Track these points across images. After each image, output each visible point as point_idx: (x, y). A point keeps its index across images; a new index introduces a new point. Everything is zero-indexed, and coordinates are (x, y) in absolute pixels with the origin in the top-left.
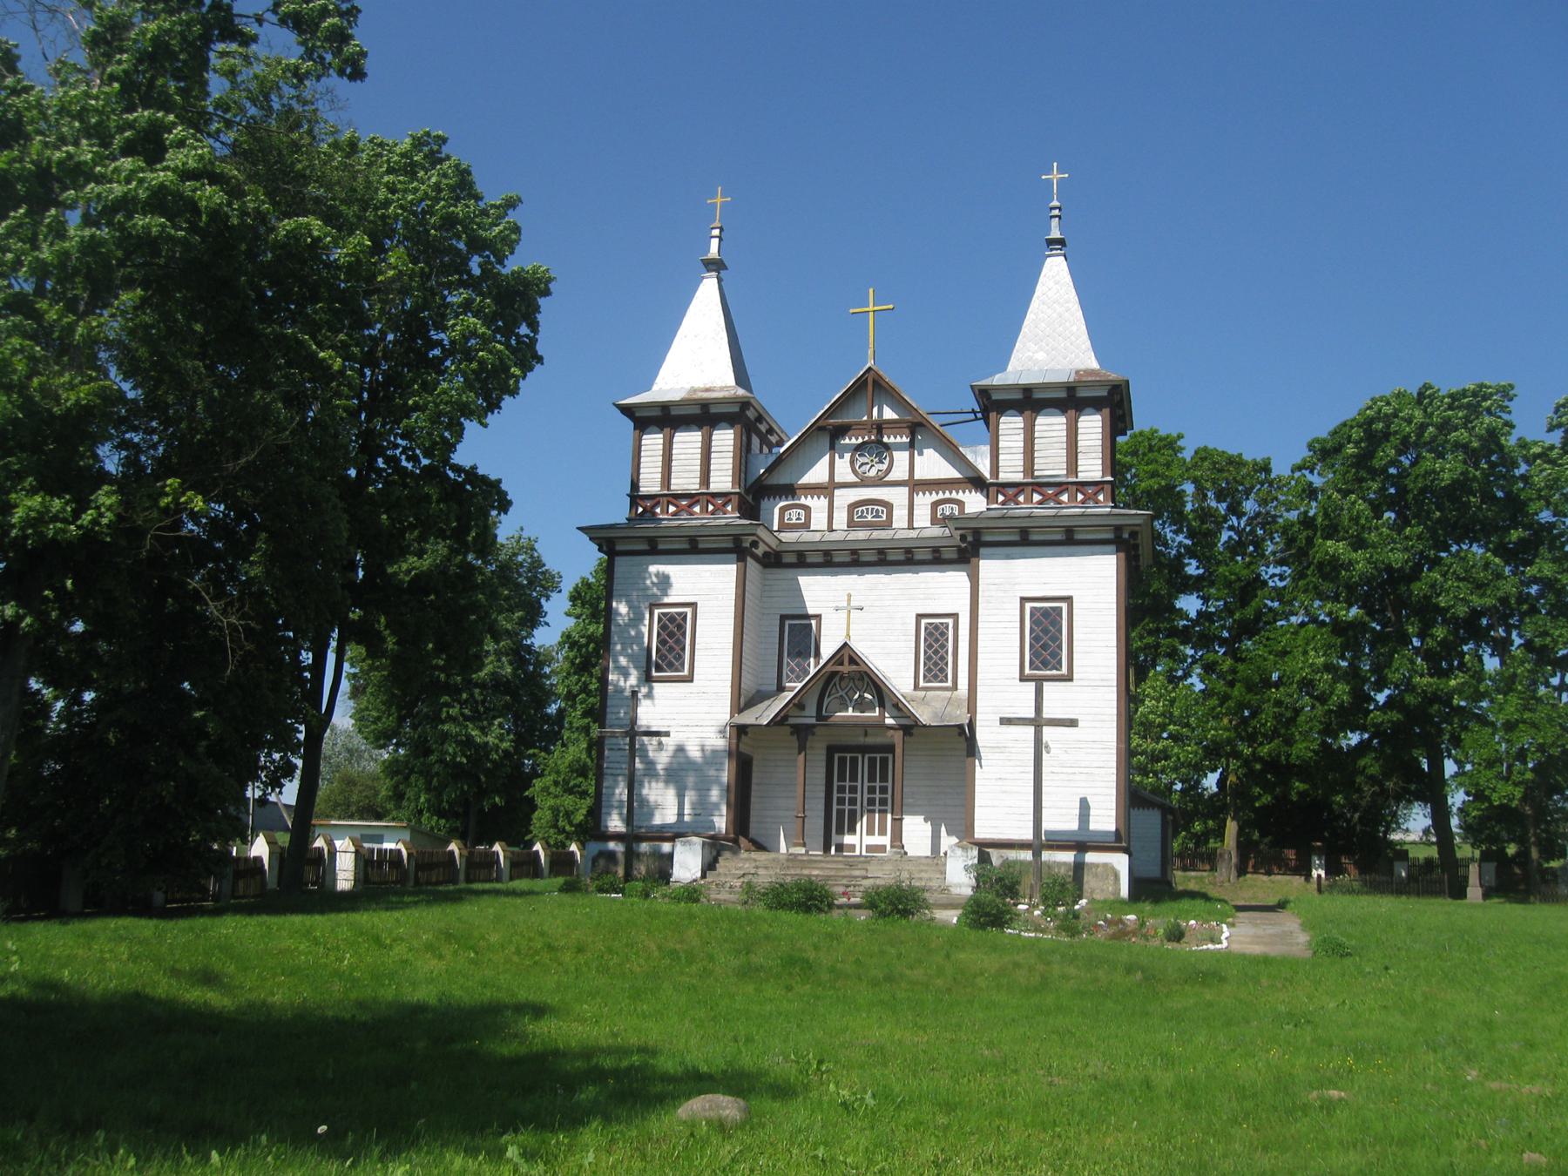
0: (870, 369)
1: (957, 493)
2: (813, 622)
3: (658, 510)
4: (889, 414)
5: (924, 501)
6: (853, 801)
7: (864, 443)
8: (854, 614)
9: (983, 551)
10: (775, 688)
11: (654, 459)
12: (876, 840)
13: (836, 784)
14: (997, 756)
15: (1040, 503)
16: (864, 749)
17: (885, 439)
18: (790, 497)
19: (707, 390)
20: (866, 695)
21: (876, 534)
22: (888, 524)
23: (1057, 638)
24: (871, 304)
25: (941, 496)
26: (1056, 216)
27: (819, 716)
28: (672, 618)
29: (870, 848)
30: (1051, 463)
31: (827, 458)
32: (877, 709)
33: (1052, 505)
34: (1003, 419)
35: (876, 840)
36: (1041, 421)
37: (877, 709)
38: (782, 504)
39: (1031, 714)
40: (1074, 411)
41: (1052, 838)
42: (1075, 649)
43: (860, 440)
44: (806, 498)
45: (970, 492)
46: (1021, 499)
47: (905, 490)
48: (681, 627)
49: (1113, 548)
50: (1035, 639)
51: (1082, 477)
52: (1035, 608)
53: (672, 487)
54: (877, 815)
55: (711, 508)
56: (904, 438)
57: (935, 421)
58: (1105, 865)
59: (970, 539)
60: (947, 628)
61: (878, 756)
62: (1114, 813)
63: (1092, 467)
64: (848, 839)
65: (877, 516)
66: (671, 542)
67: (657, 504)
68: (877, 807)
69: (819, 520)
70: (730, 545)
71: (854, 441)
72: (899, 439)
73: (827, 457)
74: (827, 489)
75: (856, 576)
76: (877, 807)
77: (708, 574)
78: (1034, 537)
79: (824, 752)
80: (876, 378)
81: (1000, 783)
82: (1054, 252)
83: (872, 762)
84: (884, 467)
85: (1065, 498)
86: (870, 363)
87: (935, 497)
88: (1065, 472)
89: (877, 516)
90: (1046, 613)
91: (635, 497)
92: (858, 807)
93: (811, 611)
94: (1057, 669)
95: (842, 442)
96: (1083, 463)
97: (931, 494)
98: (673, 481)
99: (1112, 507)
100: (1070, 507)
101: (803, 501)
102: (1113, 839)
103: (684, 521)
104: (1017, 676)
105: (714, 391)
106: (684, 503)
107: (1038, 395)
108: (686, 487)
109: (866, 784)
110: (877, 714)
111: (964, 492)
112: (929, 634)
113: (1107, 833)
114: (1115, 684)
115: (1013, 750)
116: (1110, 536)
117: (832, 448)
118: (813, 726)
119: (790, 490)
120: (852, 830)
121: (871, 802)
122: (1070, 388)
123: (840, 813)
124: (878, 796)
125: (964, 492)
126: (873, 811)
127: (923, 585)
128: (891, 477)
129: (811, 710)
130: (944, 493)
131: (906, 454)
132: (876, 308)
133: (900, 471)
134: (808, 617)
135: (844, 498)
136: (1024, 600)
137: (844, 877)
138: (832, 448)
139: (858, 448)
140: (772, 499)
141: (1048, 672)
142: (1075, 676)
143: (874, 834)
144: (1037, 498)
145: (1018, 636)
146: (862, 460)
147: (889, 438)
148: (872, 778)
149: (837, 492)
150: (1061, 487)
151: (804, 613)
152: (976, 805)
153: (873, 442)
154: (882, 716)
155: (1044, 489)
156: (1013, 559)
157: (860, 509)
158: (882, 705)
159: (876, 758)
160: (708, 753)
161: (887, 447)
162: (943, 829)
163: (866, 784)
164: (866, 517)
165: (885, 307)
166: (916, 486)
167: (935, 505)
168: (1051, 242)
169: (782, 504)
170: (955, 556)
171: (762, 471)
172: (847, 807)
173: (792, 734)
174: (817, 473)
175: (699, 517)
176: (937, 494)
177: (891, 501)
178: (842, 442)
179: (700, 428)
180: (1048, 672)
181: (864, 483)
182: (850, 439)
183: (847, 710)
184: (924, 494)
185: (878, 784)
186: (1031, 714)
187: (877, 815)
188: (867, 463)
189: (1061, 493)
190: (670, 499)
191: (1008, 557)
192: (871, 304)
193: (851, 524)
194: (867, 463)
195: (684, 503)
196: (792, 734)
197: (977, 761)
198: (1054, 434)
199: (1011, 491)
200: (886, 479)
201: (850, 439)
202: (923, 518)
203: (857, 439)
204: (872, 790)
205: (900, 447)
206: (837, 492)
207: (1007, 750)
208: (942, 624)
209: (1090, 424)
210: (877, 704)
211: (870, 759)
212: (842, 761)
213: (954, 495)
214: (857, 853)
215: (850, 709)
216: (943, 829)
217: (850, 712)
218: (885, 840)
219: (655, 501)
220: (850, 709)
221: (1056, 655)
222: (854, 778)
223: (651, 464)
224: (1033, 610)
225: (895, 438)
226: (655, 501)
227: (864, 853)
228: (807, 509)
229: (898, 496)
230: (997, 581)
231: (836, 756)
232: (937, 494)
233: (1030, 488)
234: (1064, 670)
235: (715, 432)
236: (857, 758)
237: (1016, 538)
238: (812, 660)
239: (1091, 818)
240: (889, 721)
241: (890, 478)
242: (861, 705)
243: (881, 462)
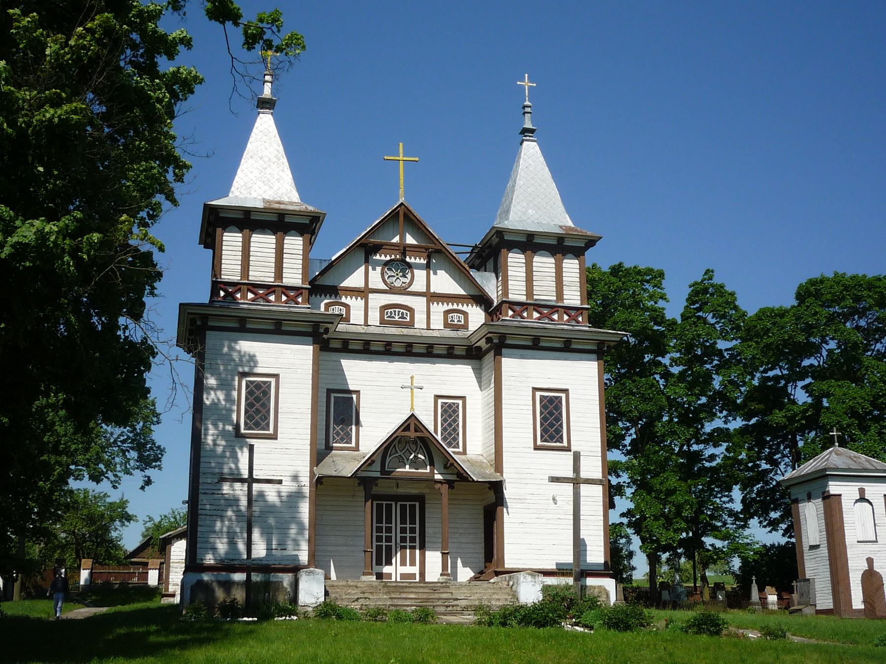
0: (402, 204)
1: (463, 305)
2: (354, 396)
3: (238, 296)
4: (410, 240)
5: (438, 309)
6: (389, 539)
7: (391, 260)
8: (415, 390)
9: (504, 351)
10: (324, 447)
11: (234, 253)
12: (408, 569)
13: (375, 525)
14: (519, 506)
15: (539, 319)
16: (397, 498)
17: (408, 259)
18: (333, 297)
19: (279, 203)
20: (420, 456)
21: (405, 331)
22: (411, 325)
23: (559, 419)
24: (401, 155)
25: (450, 307)
26: (528, 113)
27: (383, 471)
28: (258, 386)
29: (403, 576)
30: (545, 291)
31: (363, 268)
32: (428, 467)
33: (547, 321)
34: (510, 255)
35: (408, 569)
36: (537, 259)
37: (428, 467)
38: (326, 301)
39: (570, 474)
40: (530, 252)
41: (561, 567)
42: (572, 428)
43: (388, 258)
44: (346, 298)
45: (472, 306)
46: (525, 314)
48: (267, 393)
49: (594, 356)
50: (544, 419)
51: (567, 303)
52: (543, 396)
53: (250, 278)
54: (408, 551)
56: (422, 260)
57: (452, 249)
58: (600, 587)
59: (496, 341)
60: (458, 407)
62: (602, 549)
63: (573, 297)
64: (386, 569)
65: (402, 317)
66: (259, 323)
67: (239, 290)
68: (408, 544)
69: (357, 316)
70: (310, 330)
71: (383, 257)
72: (418, 261)
73: (363, 268)
74: (363, 293)
75: (387, 363)
76: (408, 544)
77: (289, 351)
78: (542, 344)
80: (406, 211)
81: (521, 526)
82: (528, 138)
83: (403, 508)
84: (407, 281)
85: (555, 317)
86: (402, 200)
87: (446, 307)
88: (555, 298)
89: (402, 317)
90: (551, 400)
91: (217, 285)
92: (393, 544)
93: (351, 388)
94: (560, 442)
95: (374, 258)
96: (566, 292)
97: (443, 304)
98: (251, 273)
99: (589, 327)
100: (560, 323)
101: (343, 300)
102: (603, 568)
103: (261, 306)
104: (532, 446)
105: (282, 204)
106: (261, 292)
107: (537, 240)
108: (262, 279)
109: (399, 526)
110: (428, 471)
111: (468, 305)
112: (444, 412)
113: (598, 565)
114: (600, 455)
115: (529, 501)
116: (594, 347)
117: (367, 261)
118: (377, 478)
119: (334, 291)
120: (389, 563)
121: (403, 539)
122: (560, 238)
124: (408, 535)
125: (468, 305)
126: (405, 548)
127: (438, 373)
128: (412, 289)
129: (377, 466)
130: (453, 305)
131: (424, 273)
132: (405, 159)
133: (419, 285)
134: (350, 392)
135: (377, 301)
136: (535, 389)
137: (439, 599)
138: (367, 261)
139: (386, 264)
140: (318, 296)
141: (554, 444)
143: (406, 566)
144: (536, 315)
145: (531, 416)
146: (390, 273)
147: (410, 258)
148: (403, 521)
149: (371, 296)
150: (554, 308)
151: (346, 388)
152: (505, 542)
153: (398, 260)
154: (433, 473)
155: (541, 309)
156: (526, 358)
157: (390, 310)
158: (432, 464)
160: (284, 499)
161: (410, 266)
162: (459, 561)
163: (399, 526)
164: (395, 318)
165: (391, 158)
166: (433, 297)
167: (447, 313)
168: (525, 131)
169: (326, 301)
170: (464, 353)
171: (317, 273)
172: (384, 544)
173: (359, 484)
174: (355, 280)
175: (277, 304)
176: (448, 304)
177: (413, 307)
178: (374, 258)
179: (241, 230)
180: (554, 444)
181: (392, 290)
182: (381, 256)
183: (405, 467)
184: (438, 304)
185: (408, 526)
186: (570, 474)
187: (408, 551)
188: (394, 276)
189: (553, 313)
190: (250, 287)
191: (522, 357)
192: (401, 155)
193: (383, 322)
194: (394, 276)
195: (261, 292)
196: (359, 484)
197: (505, 509)
198: (547, 270)
199: (518, 308)
200: (408, 290)
201: (381, 256)
202: (437, 322)
203: (386, 256)
204: (403, 530)
205: (419, 267)
206: (371, 296)
207: (527, 501)
208: (454, 404)
209: (570, 266)
210: (428, 463)
213: (460, 307)
214: (393, 579)
215: (407, 466)
216: (459, 561)
217: (407, 469)
218: (415, 570)
219: (237, 288)
220: (407, 466)
221: (559, 431)
222: (389, 521)
223: (231, 257)
225: (415, 259)
226: (237, 288)
227: (398, 580)
228: (347, 307)
229: (419, 304)
230: (515, 374)
232: (448, 304)
233: (532, 307)
234: (565, 444)
235: (253, 235)
237: (530, 343)
238: (354, 427)
239: (588, 553)
240: (438, 477)
242: (415, 464)
243: (404, 276)
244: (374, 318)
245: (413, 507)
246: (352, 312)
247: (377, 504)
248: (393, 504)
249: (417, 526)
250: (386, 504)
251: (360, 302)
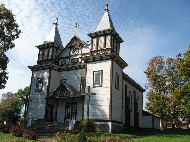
30: (101, 46)
42: (103, 80)
55: (48, 61)
69: (67, 63)
79: (65, 104)
123: (67, 115)
128: (79, 54)
141: (98, 85)
142: (103, 86)
180: (98, 85)
212: (68, 105)
222: (70, 109)
224: (95, 73)
228: (65, 61)
230: (90, 69)
231: (67, 104)
241: (79, 54)
244: (71, 61)
245: (75, 105)
246: (66, 62)
249: (75, 110)
251: (68, 60)
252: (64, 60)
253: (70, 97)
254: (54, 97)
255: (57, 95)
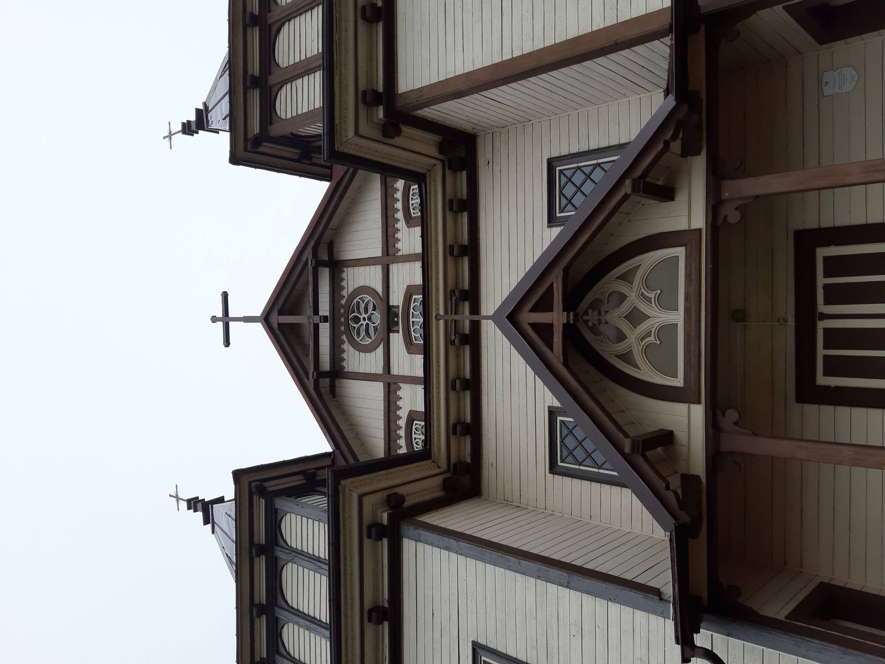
25: (400, 215)
43: (344, 337)
47: (394, 269)
61: (821, 281)
83: (835, 295)
87: (401, 225)
110: (680, 252)
128: (379, 288)
159: (826, 287)
188: (367, 325)
206: (395, 371)
211: (827, 302)
212: (834, 367)
231: (822, 380)
236: (826, 331)
245: (834, 266)
247: (826, 374)
248: (822, 325)
250: (826, 347)
252: (402, 423)
253: (699, 221)
254: (689, 480)
255: (666, 438)
